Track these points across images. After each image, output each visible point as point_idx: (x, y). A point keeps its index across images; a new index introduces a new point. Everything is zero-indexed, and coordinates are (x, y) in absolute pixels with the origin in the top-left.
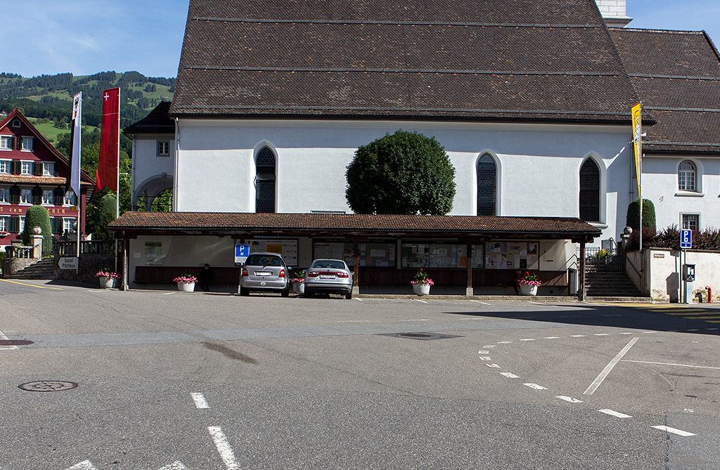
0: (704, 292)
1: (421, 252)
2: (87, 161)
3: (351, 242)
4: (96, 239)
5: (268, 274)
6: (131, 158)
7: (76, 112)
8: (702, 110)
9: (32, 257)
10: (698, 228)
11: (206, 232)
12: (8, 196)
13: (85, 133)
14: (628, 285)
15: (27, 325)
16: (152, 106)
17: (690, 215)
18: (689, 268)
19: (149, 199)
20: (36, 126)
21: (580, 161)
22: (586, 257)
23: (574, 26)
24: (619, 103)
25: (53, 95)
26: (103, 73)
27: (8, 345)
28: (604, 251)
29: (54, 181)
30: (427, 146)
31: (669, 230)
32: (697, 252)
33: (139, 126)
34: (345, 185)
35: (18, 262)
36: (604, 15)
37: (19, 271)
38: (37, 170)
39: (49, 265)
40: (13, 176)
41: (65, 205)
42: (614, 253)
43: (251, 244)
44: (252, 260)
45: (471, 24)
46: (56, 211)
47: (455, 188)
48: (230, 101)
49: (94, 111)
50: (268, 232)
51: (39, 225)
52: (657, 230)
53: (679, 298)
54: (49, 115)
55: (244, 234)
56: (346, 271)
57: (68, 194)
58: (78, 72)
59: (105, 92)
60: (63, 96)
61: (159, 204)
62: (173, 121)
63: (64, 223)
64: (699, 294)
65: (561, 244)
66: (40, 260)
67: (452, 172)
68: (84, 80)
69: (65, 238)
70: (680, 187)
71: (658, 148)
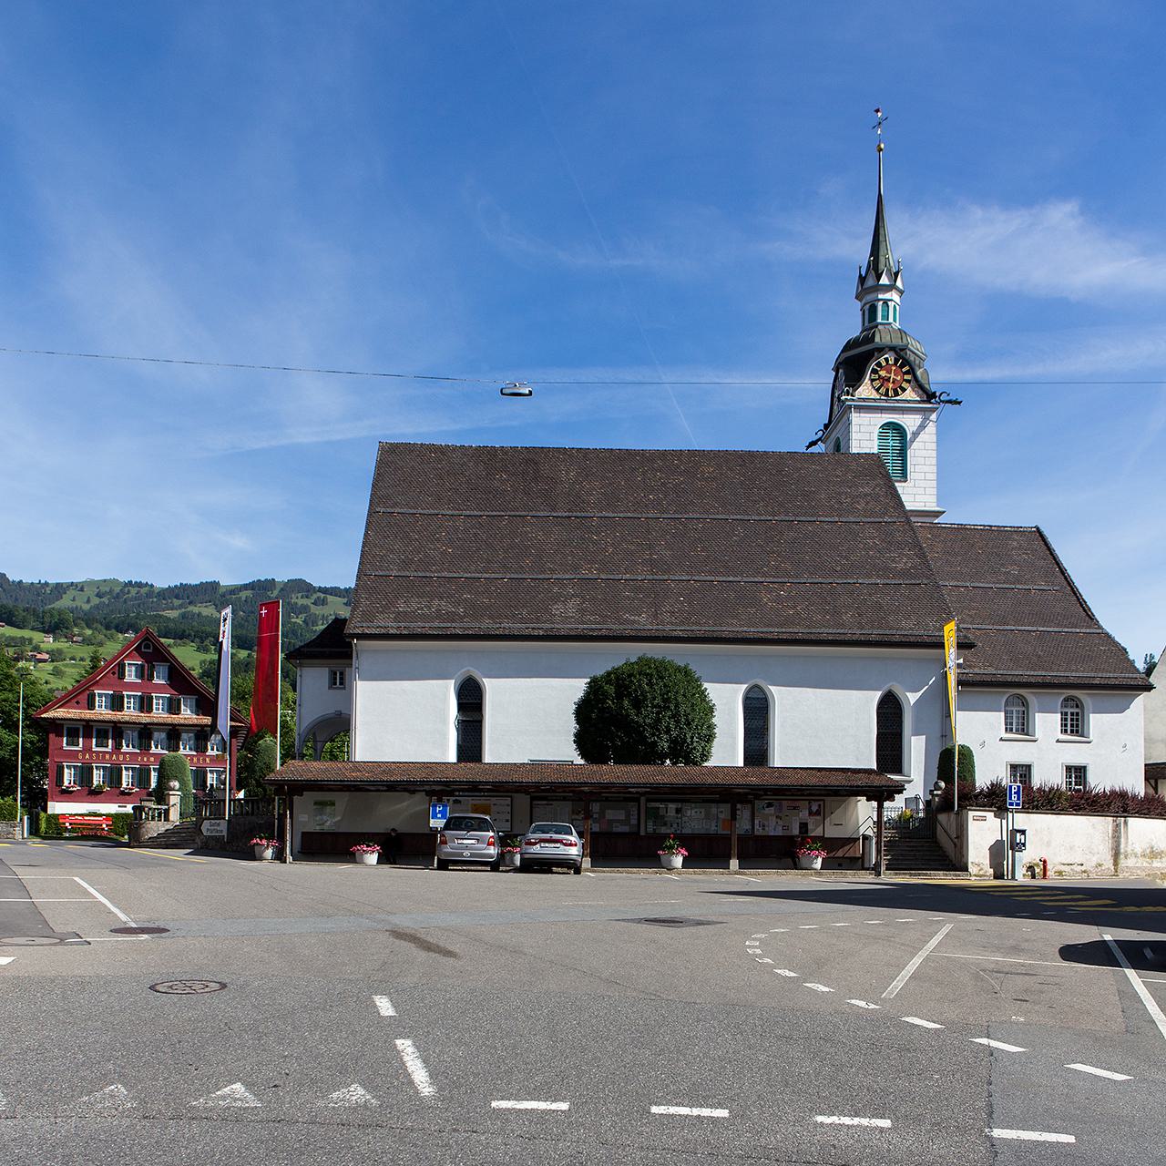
0: (1038, 865)
1: (672, 813)
2: (238, 696)
3: (581, 800)
4: (250, 796)
5: (473, 842)
6: (295, 690)
7: (224, 632)
8: (1035, 629)
9: (167, 819)
10: (1030, 781)
11: (392, 787)
12: (165, 741)
13: (236, 659)
14: (939, 856)
15: (162, 908)
16: (322, 624)
17: (1020, 765)
18: (1018, 834)
19: (319, 745)
20: (172, 651)
21: (877, 695)
22: (885, 819)
23: (869, 520)
24: (928, 620)
25: (195, 609)
26: (259, 581)
27: (137, 933)
28: (908, 813)
29: (195, 722)
30: (679, 676)
31: (992, 785)
32: (1028, 813)
33: (306, 650)
34: (572, 726)
35: (149, 826)
36: (909, 506)
37: (150, 838)
38: (173, 707)
39: (189, 830)
40: (143, 715)
41: (210, 752)
42: (921, 815)
43: (451, 802)
44: (453, 824)
45: (735, 517)
46: (198, 760)
47: (715, 731)
48: (424, 618)
49: (247, 630)
50: (473, 788)
51: (176, 778)
52: (977, 785)
53: (1006, 873)
54: (190, 635)
55: (442, 790)
56: (573, 838)
57: (214, 739)
58: (227, 580)
59: (262, 606)
60: (208, 611)
61: (331, 751)
62: (350, 645)
63: (209, 775)
64: (1031, 868)
65: (852, 805)
66: (178, 823)
67: (711, 709)
68: (235, 590)
69: (210, 794)
70: (1006, 729)
71: (978, 678)
